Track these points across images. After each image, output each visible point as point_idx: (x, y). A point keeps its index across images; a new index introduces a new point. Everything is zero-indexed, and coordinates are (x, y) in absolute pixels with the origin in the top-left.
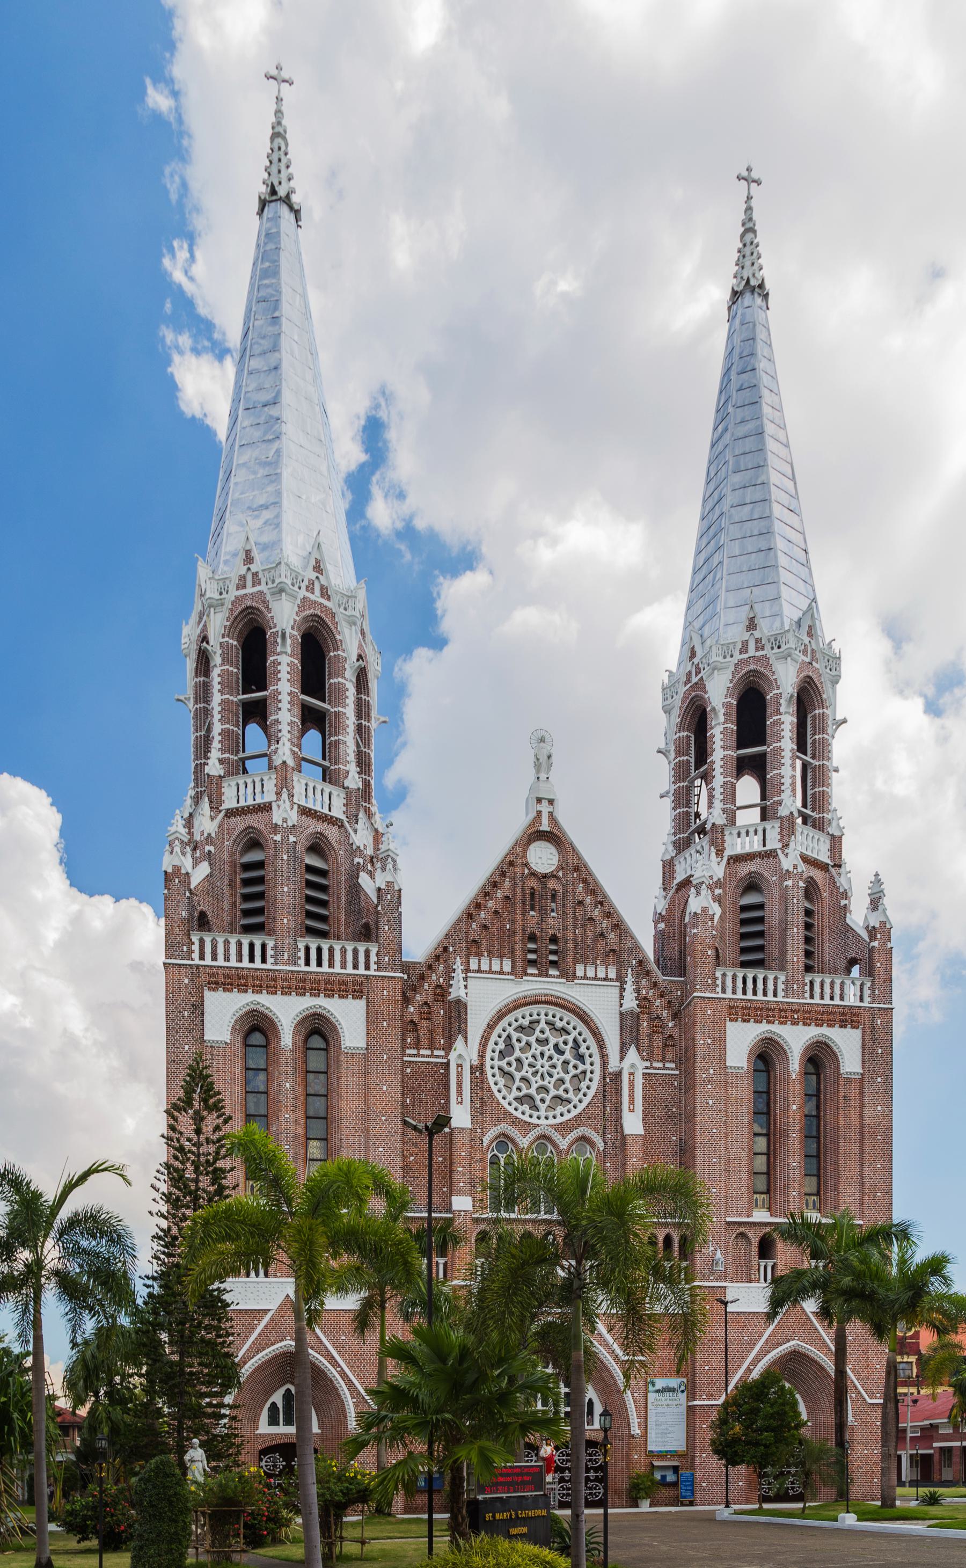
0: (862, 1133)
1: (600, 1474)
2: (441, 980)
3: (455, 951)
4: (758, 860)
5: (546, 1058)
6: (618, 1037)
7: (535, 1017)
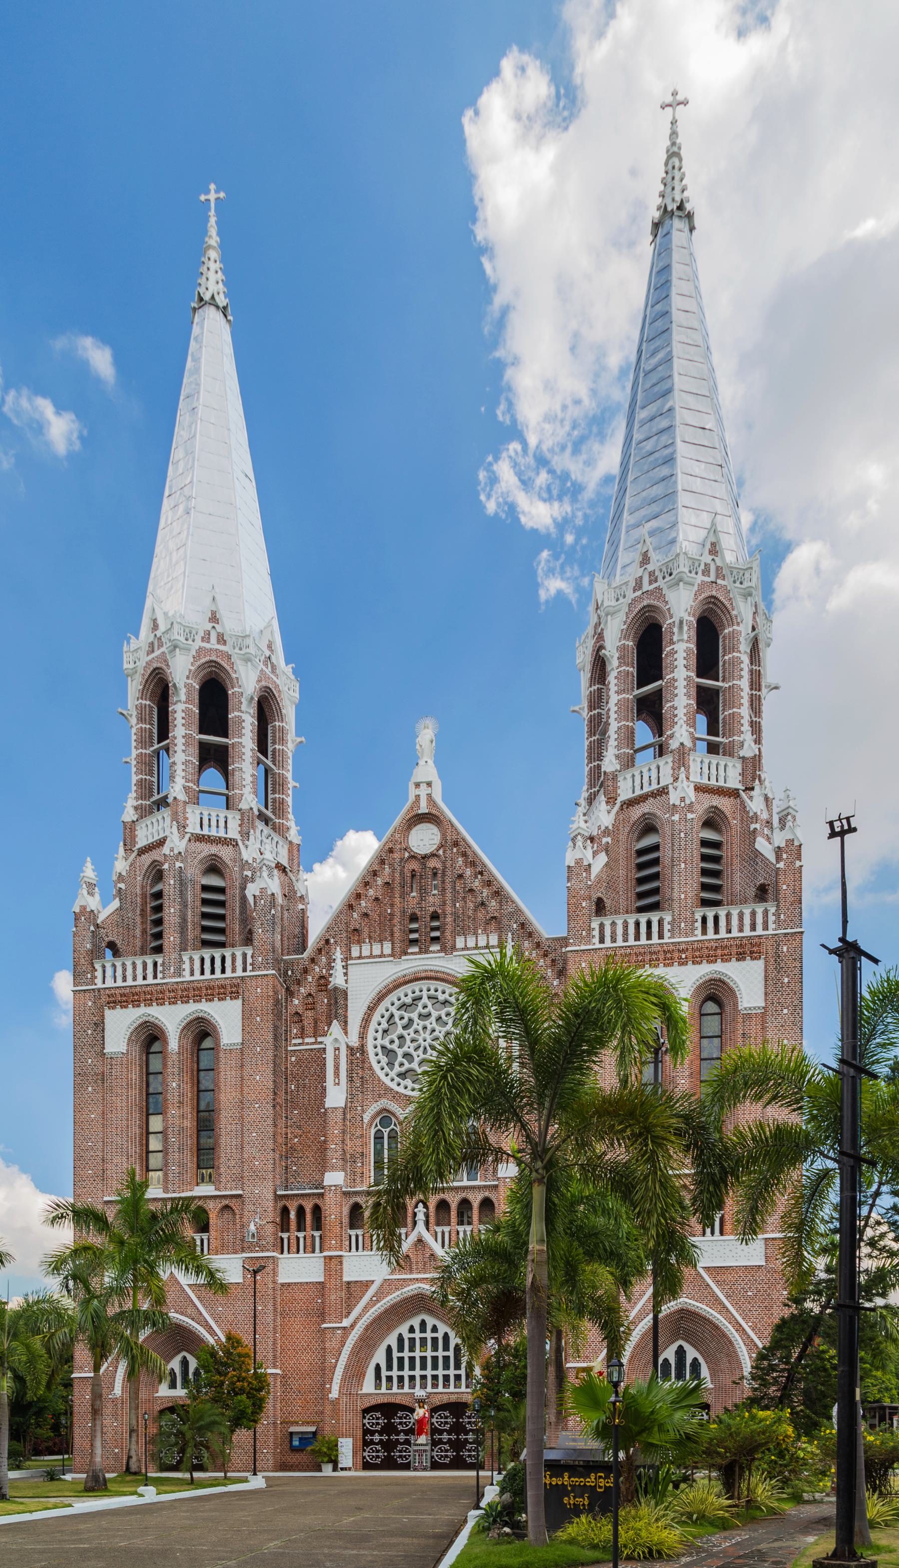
2: (324, 971)
3: (336, 942)
4: (651, 800)
5: (428, 1032)
7: (418, 993)
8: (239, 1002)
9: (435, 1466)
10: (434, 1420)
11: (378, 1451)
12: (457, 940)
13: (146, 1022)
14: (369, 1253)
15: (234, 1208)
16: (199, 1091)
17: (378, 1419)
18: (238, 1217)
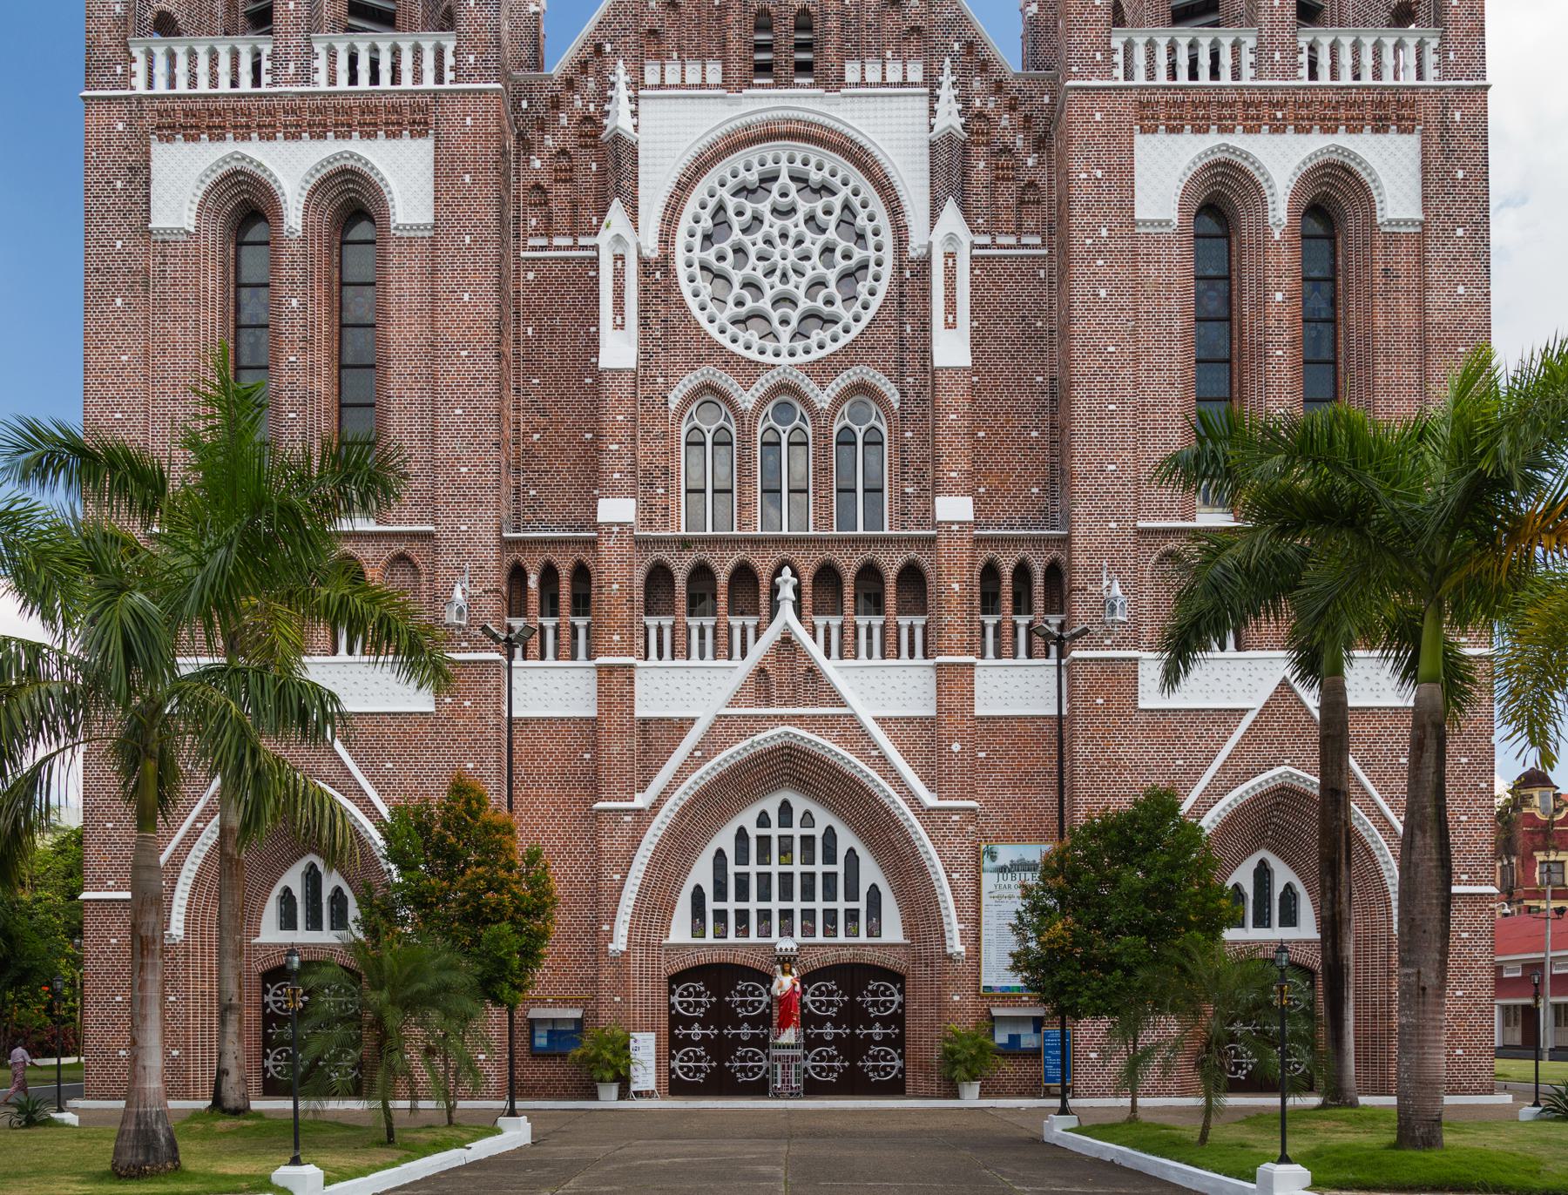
0: (1424, 343)
1: (893, 1031)
3: (615, 51)
6: (927, 190)
8: (426, 146)
9: (813, 1088)
10: (807, 998)
11: (699, 1059)
12: (847, 67)
13: (237, 173)
14: (684, 663)
15: (417, 560)
16: (342, 326)
17: (699, 994)
18: (424, 578)
